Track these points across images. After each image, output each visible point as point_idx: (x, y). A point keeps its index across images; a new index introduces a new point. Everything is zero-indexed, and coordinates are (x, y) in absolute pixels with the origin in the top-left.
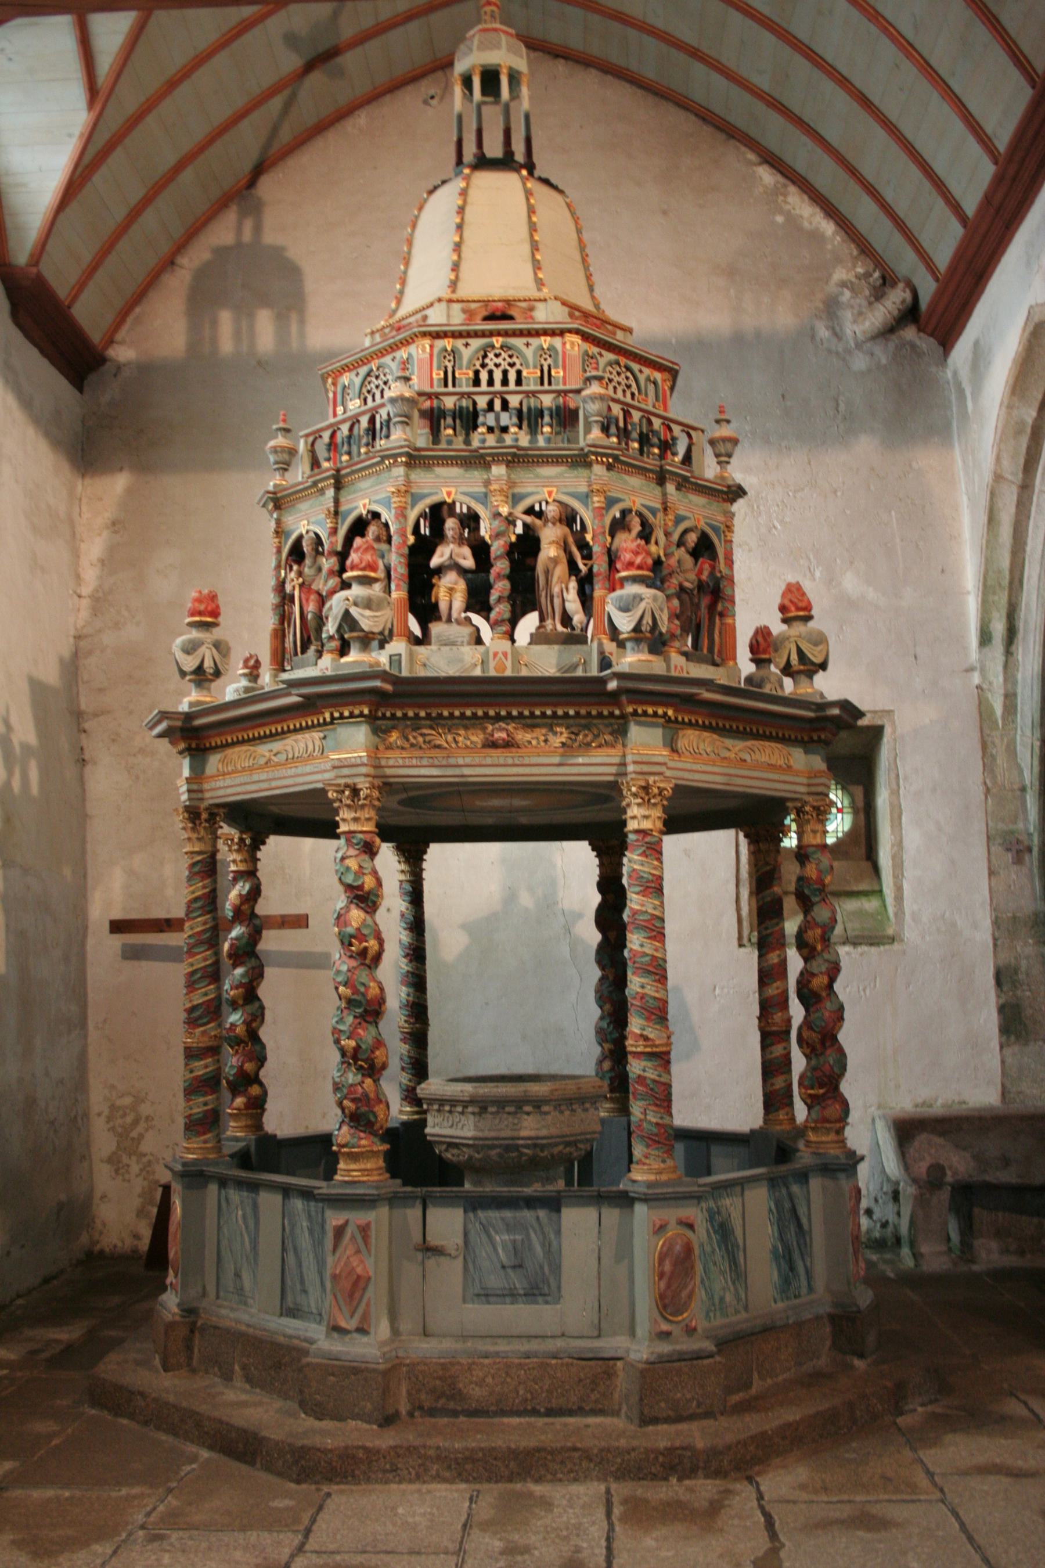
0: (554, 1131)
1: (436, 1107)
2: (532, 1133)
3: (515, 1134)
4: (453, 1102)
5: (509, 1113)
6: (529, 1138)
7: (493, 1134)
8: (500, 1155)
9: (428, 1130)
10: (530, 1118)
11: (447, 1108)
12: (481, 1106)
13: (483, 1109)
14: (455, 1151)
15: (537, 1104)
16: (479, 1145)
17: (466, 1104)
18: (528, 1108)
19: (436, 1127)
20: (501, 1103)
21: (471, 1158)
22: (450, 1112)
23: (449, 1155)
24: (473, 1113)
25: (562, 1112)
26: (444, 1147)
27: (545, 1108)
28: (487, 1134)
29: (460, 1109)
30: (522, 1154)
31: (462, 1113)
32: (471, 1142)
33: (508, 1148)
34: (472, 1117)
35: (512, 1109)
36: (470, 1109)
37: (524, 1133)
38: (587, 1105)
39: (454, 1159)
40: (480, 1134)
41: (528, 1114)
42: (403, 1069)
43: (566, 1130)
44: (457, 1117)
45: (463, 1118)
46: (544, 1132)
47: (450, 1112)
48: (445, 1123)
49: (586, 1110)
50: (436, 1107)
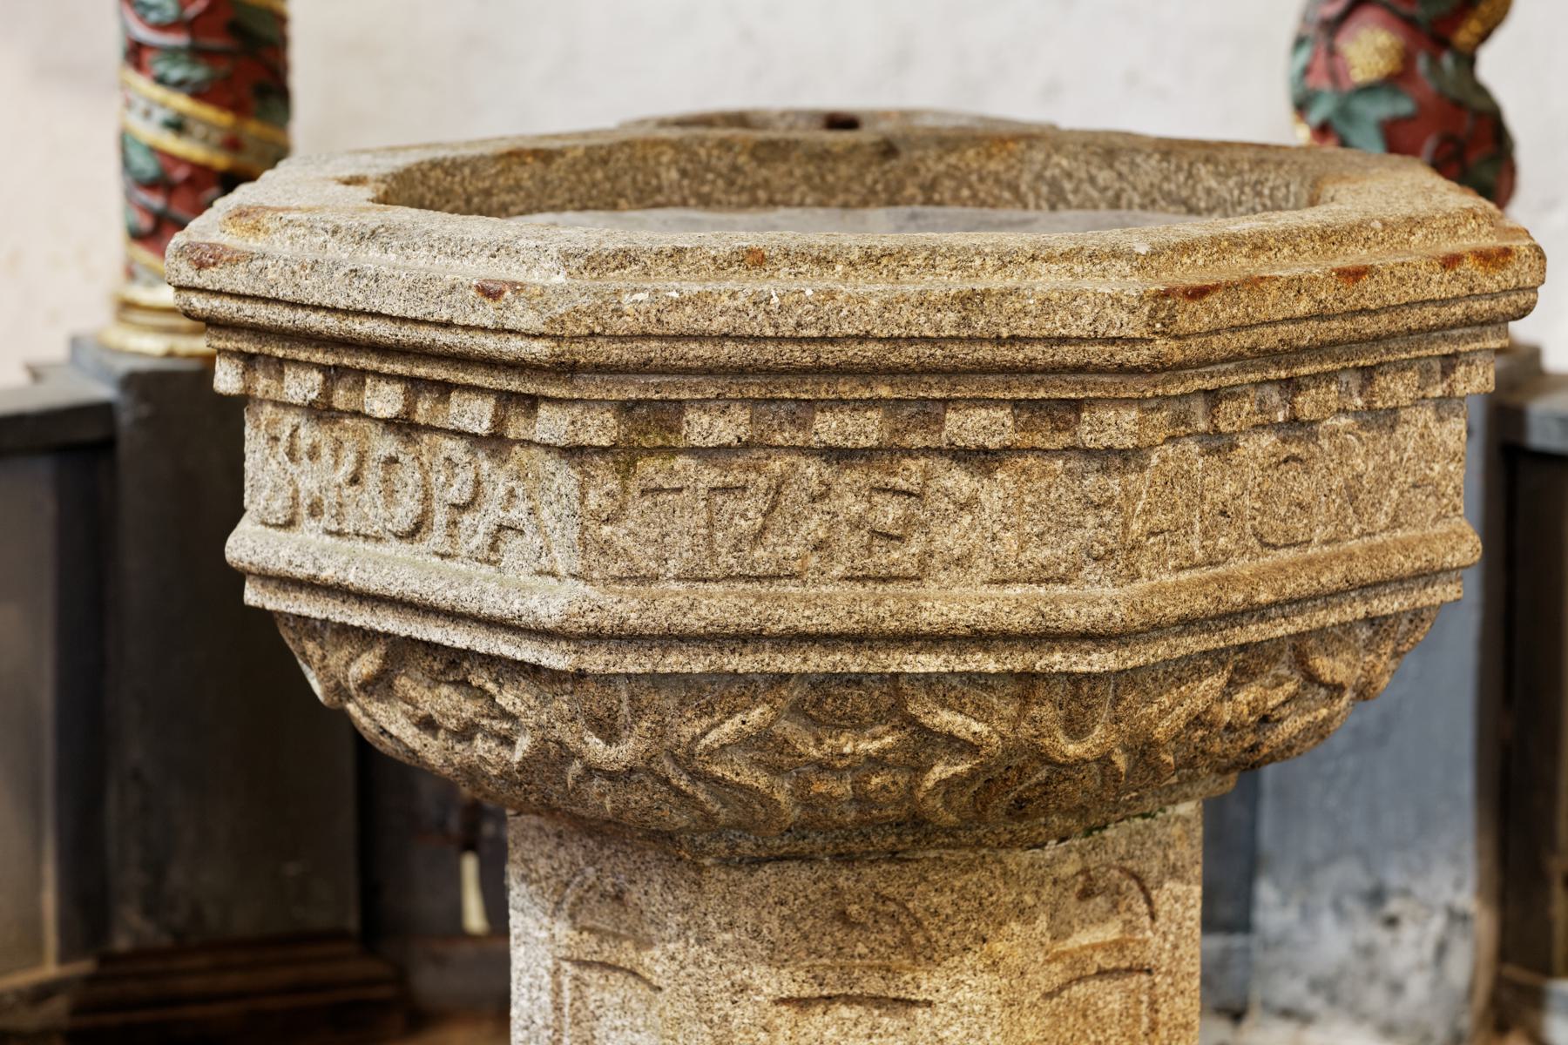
0: (1166, 586)
1: (302, 386)
2: (1012, 606)
3: (883, 607)
4: (429, 365)
5: (838, 455)
6: (981, 639)
7: (720, 605)
8: (759, 743)
9: (246, 544)
10: (995, 492)
11: (384, 401)
12: (635, 397)
13: (650, 426)
14: (445, 701)
15: (1051, 388)
16: (603, 670)
17: (523, 383)
18: (971, 425)
19: (309, 523)
20: (785, 378)
21: (552, 757)
22: (404, 426)
23: (389, 722)
24: (574, 452)
25: (1219, 444)
26: (366, 664)
27: (1115, 426)
28: (673, 603)
29: (476, 414)
30: (930, 742)
31: (495, 442)
32: (556, 658)
33: (824, 701)
34: (565, 478)
35: (868, 429)
36: (551, 424)
37: (945, 603)
38: (1397, 389)
39: (432, 750)
40: (625, 607)
41: (981, 459)
42: (136, 53)
43: (1250, 572)
44: (450, 469)
45: (499, 481)
46: (1098, 598)
47: (404, 426)
48: (368, 507)
49: (1384, 419)
50: (302, 386)
